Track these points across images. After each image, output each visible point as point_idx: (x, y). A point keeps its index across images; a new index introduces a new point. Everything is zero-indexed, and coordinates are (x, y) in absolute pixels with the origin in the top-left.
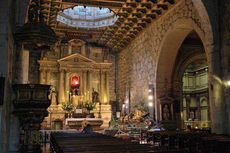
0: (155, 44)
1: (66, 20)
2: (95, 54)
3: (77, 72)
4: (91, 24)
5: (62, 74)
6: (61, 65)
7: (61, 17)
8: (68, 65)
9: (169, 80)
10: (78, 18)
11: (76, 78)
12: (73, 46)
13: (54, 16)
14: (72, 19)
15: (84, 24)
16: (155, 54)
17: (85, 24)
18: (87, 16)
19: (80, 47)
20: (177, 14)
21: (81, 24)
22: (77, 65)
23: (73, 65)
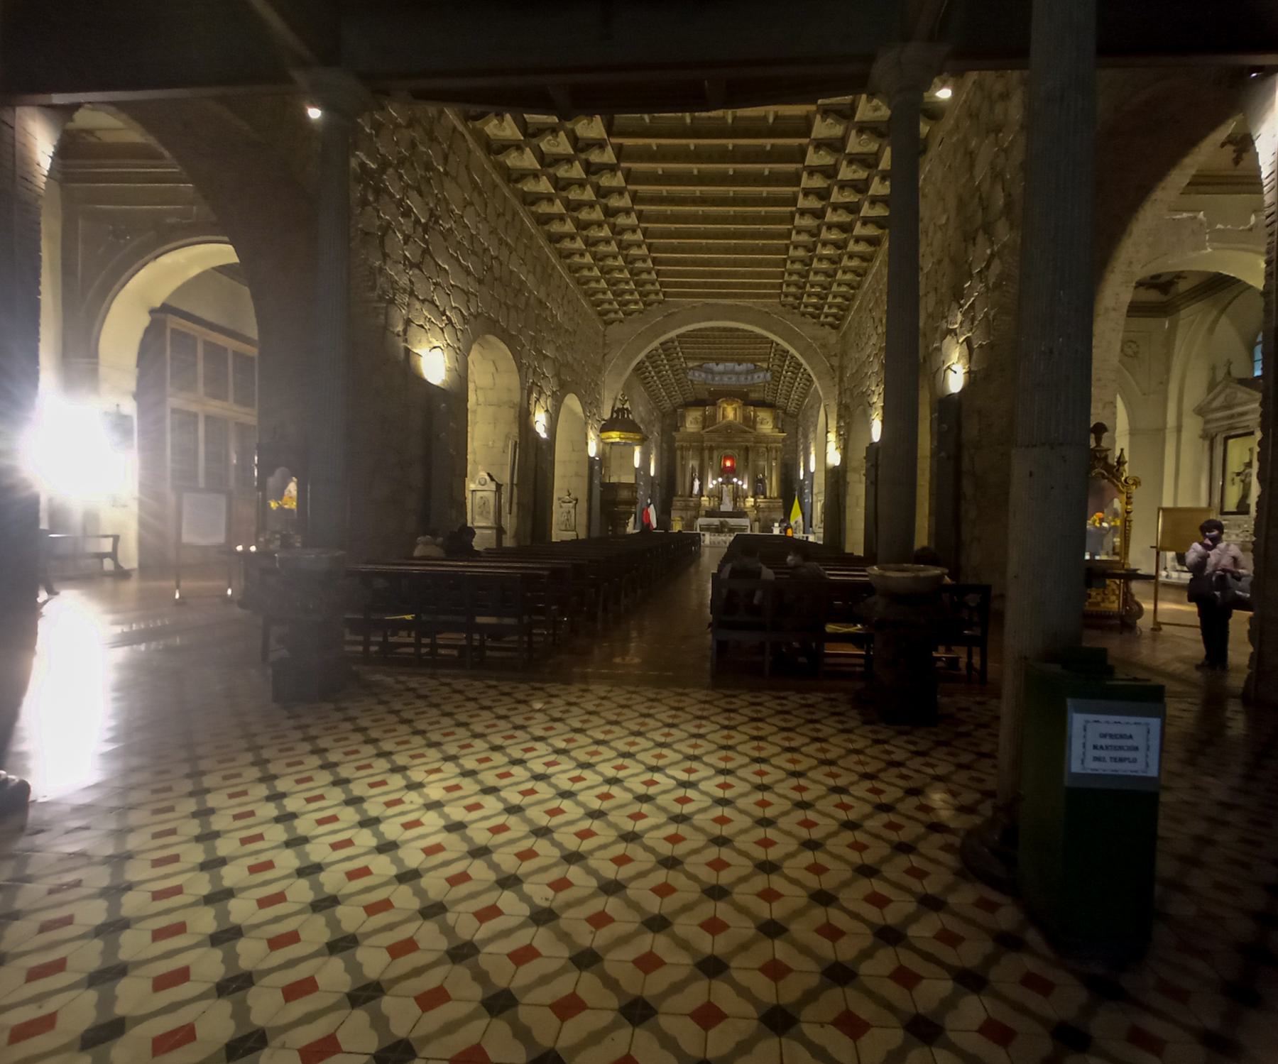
3: (731, 448)
17: (734, 379)
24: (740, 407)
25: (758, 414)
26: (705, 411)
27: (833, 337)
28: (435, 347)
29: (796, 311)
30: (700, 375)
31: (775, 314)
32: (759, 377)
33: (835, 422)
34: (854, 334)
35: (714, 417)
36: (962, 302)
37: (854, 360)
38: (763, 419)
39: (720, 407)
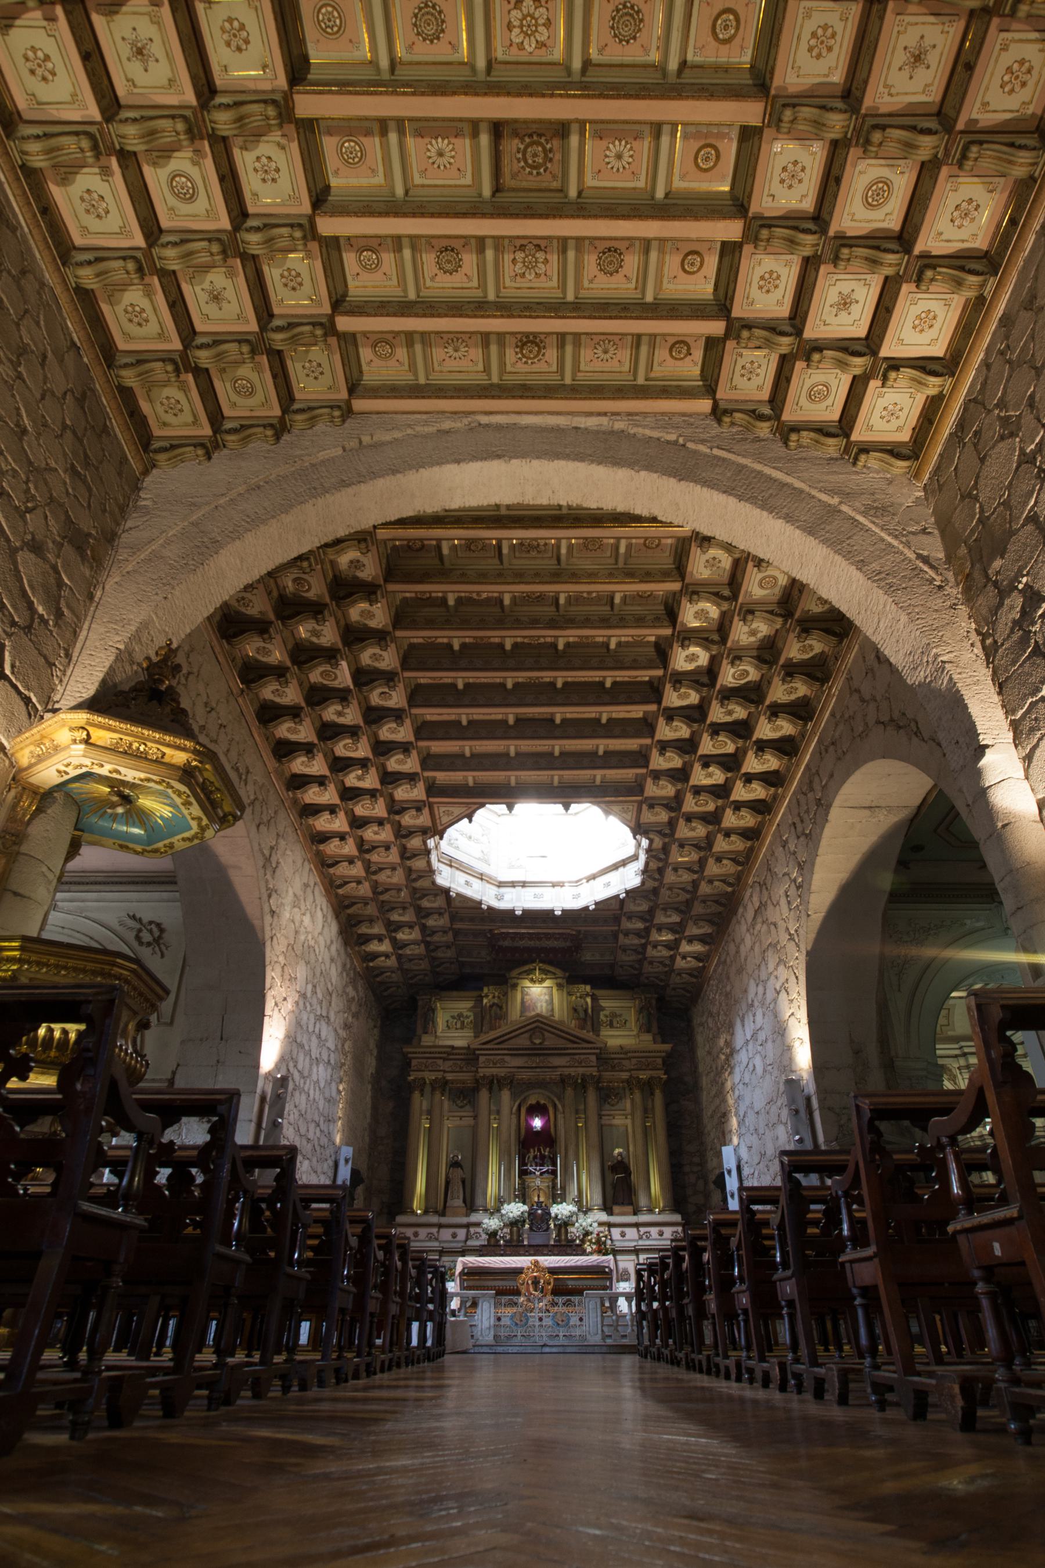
0: (785, 914)
5: (484, 1095)
6: (482, 1059)
7: (458, 873)
8: (507, 1058)
9: (872, 1052)
11: (537, 1110)
13: (419, 864)
16: (791, 947)
20: (831, 749)
23: (525, 1059)
24: (560, 986)
25: (603, 1003)
26: (480, 999)
33: (1000, 713)
35: (499, 1011)
38: (614, 1015)
39: (515, 986)
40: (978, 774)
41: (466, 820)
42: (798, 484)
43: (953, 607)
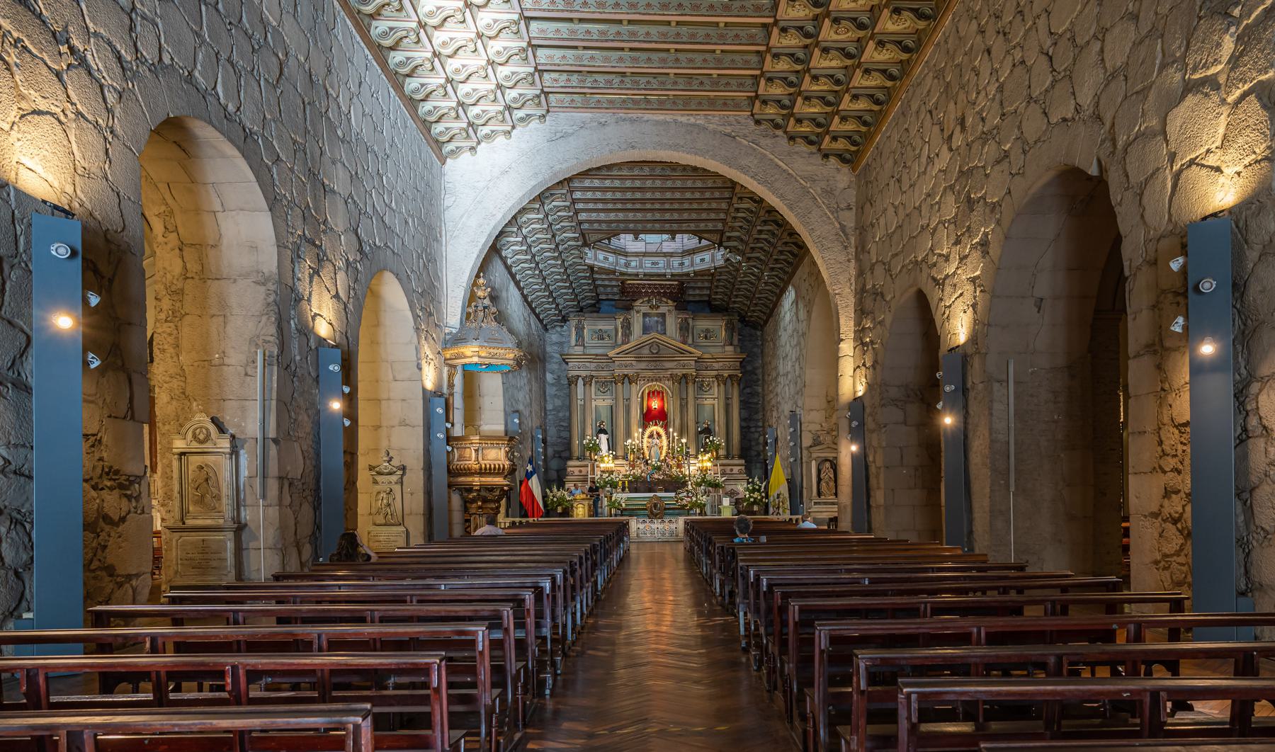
1: (611, 258)
2: (702, 331)
4: (676, 264)
10: (644, 250)
12: (645, 315)
14: (627, 253)
15: (657, 263)
18: (664, 244)
19: (663, 315)
21: (650, 265)
22: (658, 363)
27: (843, 177)
28: (35, 112)
29: (779, 132)
30: (606, 259)
31: (745, 137)
32: (702, 260)
34: (891, 162)
36: (1236, 12)
37: (891, 210)
40: (838, 350)
41: (607, 241)
42: (791, 171)
43: (849, 261)
